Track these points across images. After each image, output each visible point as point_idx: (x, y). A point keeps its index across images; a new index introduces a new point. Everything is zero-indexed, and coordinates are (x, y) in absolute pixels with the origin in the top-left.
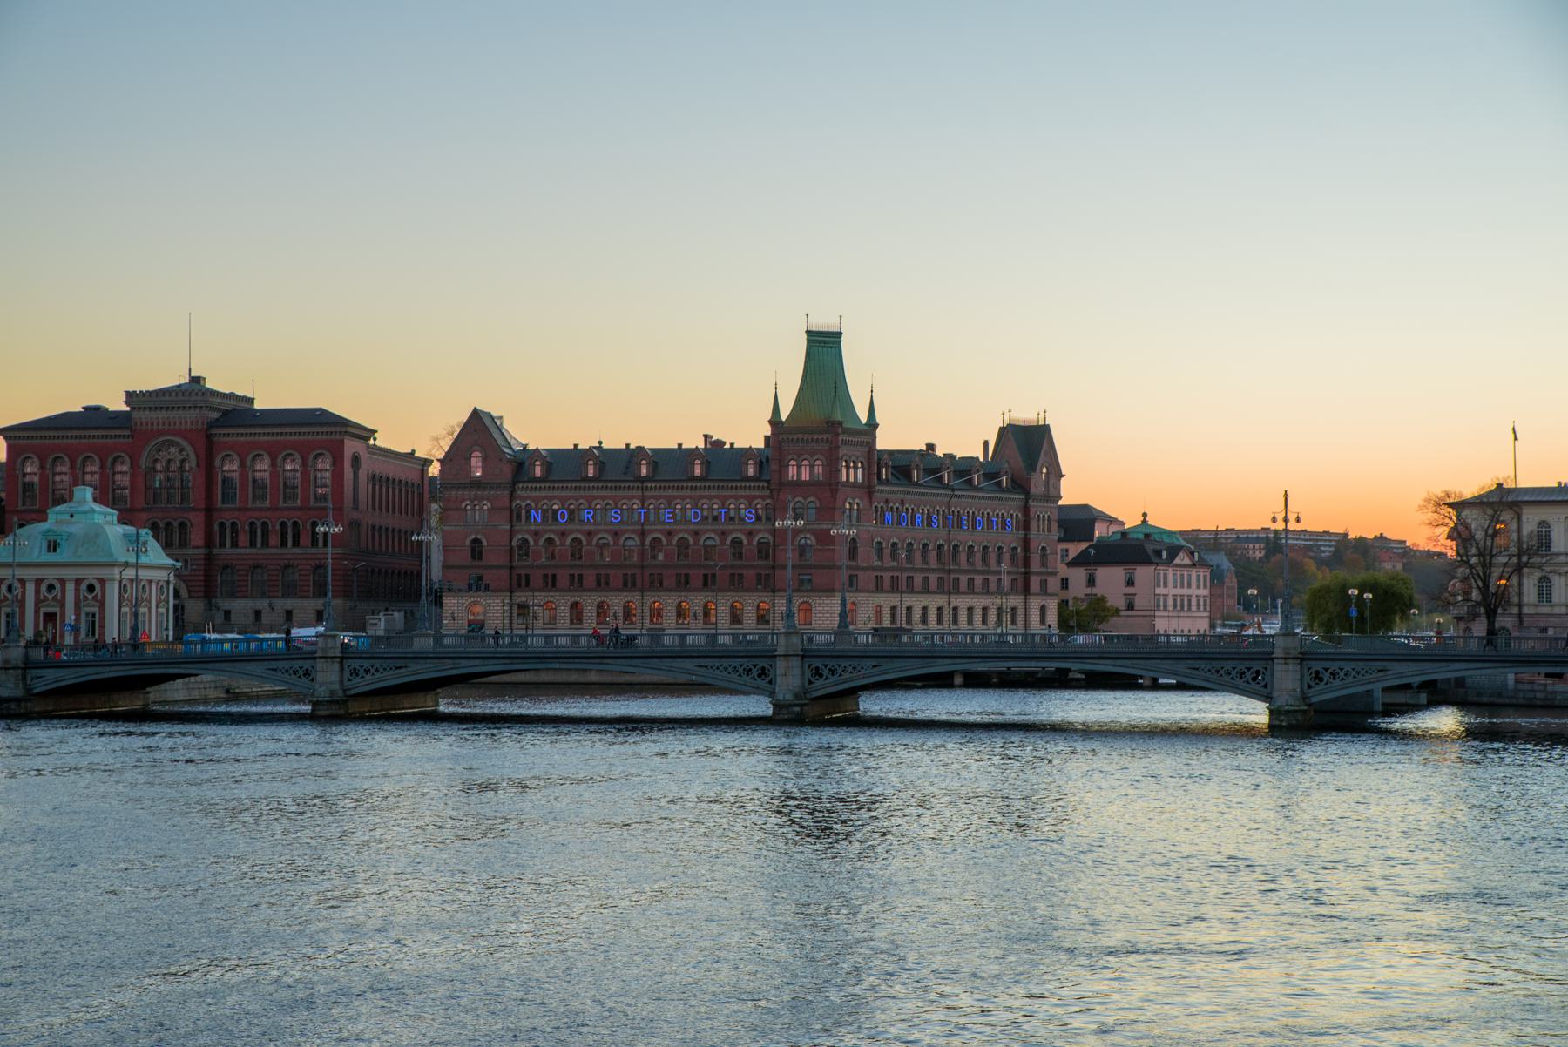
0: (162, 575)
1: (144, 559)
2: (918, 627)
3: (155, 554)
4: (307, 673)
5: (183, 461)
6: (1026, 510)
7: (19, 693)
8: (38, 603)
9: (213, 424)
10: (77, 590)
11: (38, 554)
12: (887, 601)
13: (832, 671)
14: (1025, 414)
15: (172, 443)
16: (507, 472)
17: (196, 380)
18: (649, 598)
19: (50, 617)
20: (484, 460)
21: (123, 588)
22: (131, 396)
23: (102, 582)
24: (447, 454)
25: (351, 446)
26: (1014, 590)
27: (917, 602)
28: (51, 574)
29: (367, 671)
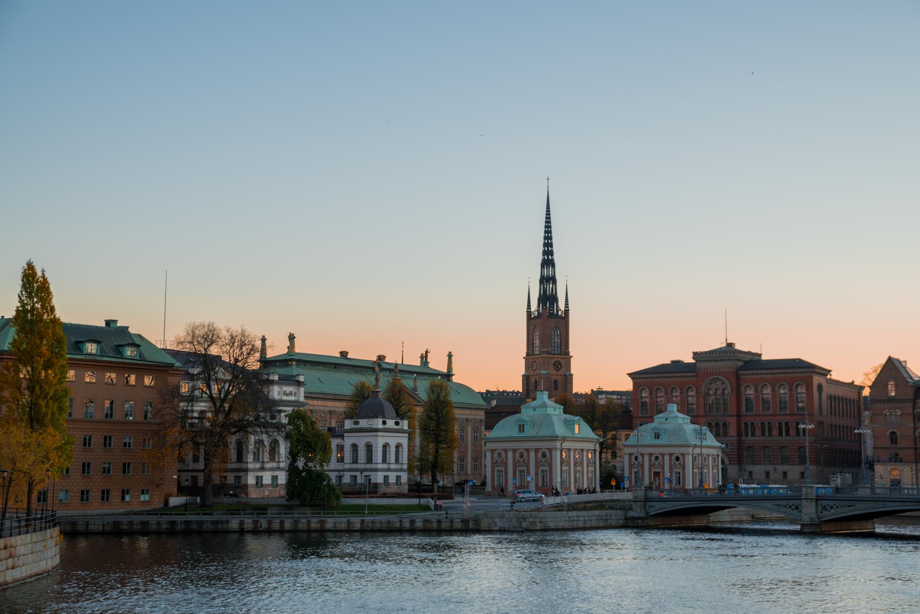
0: (714, 452)
1: (704, 443)
3: (711, 440)
4: (797, 508)
5: (724, 389)
7: (643, 515)
8: (651, 466)
9: (739, 369)
10: (670, 459)
11: (649, 439)
15: (718, 380)
16: (910, 393)
17: (730, 345)
19: (657, 474)
20: (896, 386)
21: (694, 459)
22: (696, 355)
23: (683, 455)
24: (874, 383)
25: (816, 380)
28: (656, 451)
29: (832, 508)
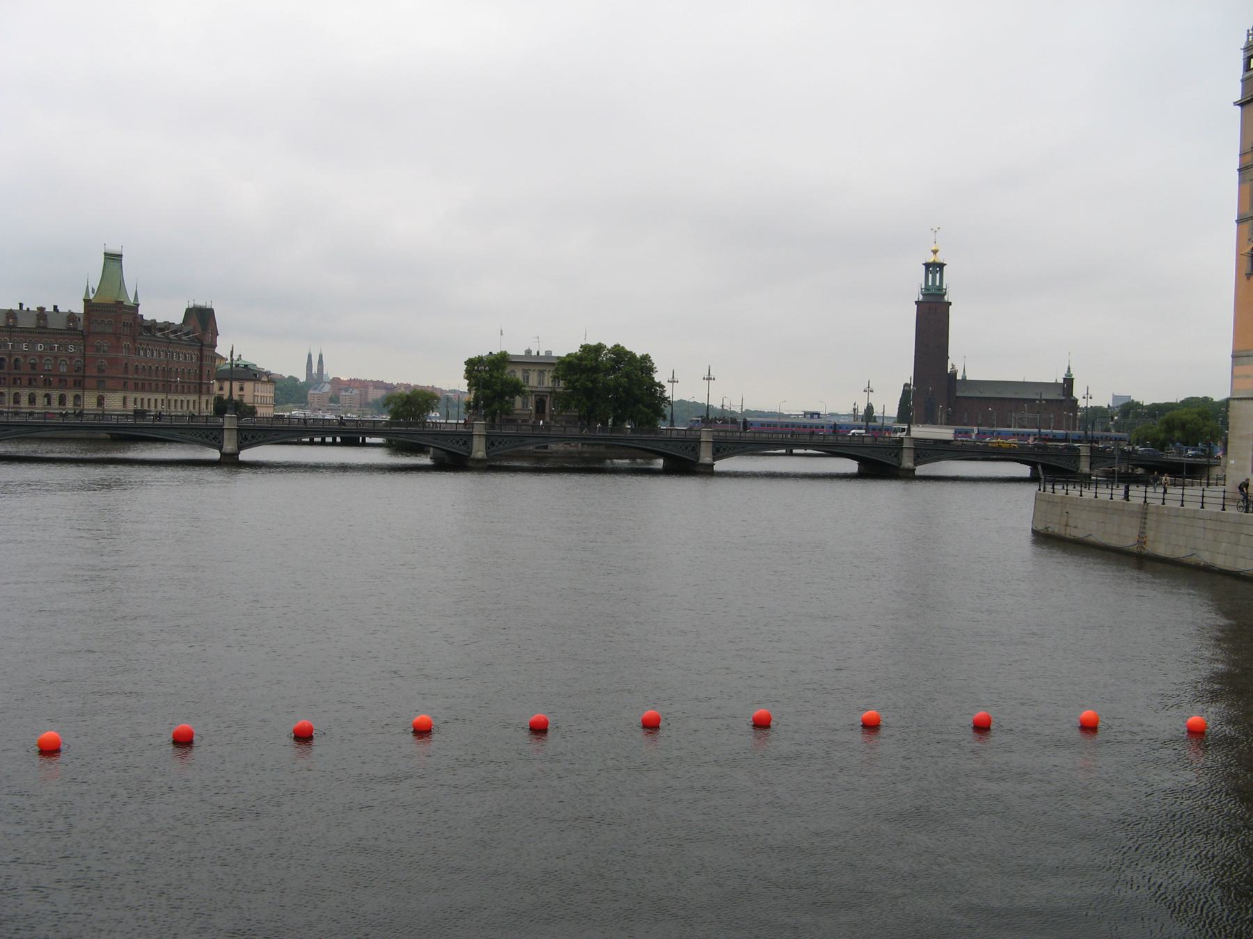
2: (152, 408)
6: (201, 351)
12: (139, 396)
13: (253, 437)
14: (201, 302)
18: (13, 391)
26: (195, 392)
27: (153, 397)
